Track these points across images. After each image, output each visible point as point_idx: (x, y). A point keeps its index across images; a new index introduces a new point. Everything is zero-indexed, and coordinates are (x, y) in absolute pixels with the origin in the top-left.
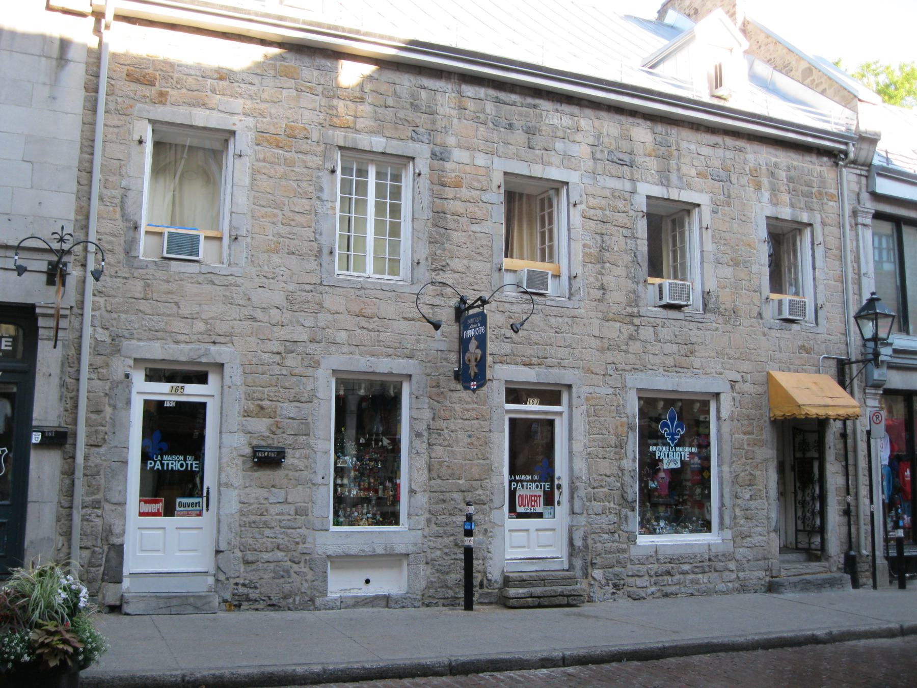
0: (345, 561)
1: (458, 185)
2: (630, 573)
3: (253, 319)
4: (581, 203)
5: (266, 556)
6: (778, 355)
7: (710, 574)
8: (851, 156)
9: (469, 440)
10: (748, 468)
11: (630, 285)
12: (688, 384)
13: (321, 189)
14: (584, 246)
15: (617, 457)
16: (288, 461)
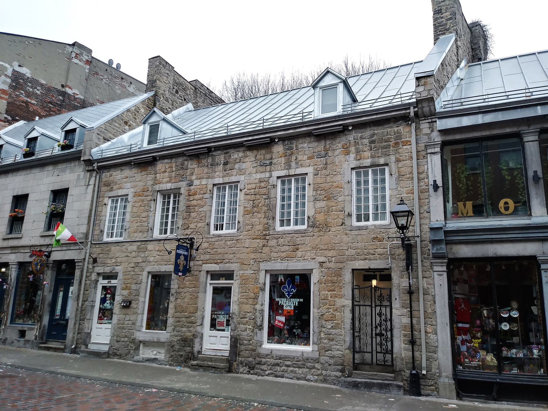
1: (195, 194)
4: (245, 189)
5: (122, 339)
6: (356, 245)
7: (304, 369)
10: (331, 310)
11: (265, 221)
12: (295, 265)
13: (151, 208)
14: (245, 207)
16: (132, 305)
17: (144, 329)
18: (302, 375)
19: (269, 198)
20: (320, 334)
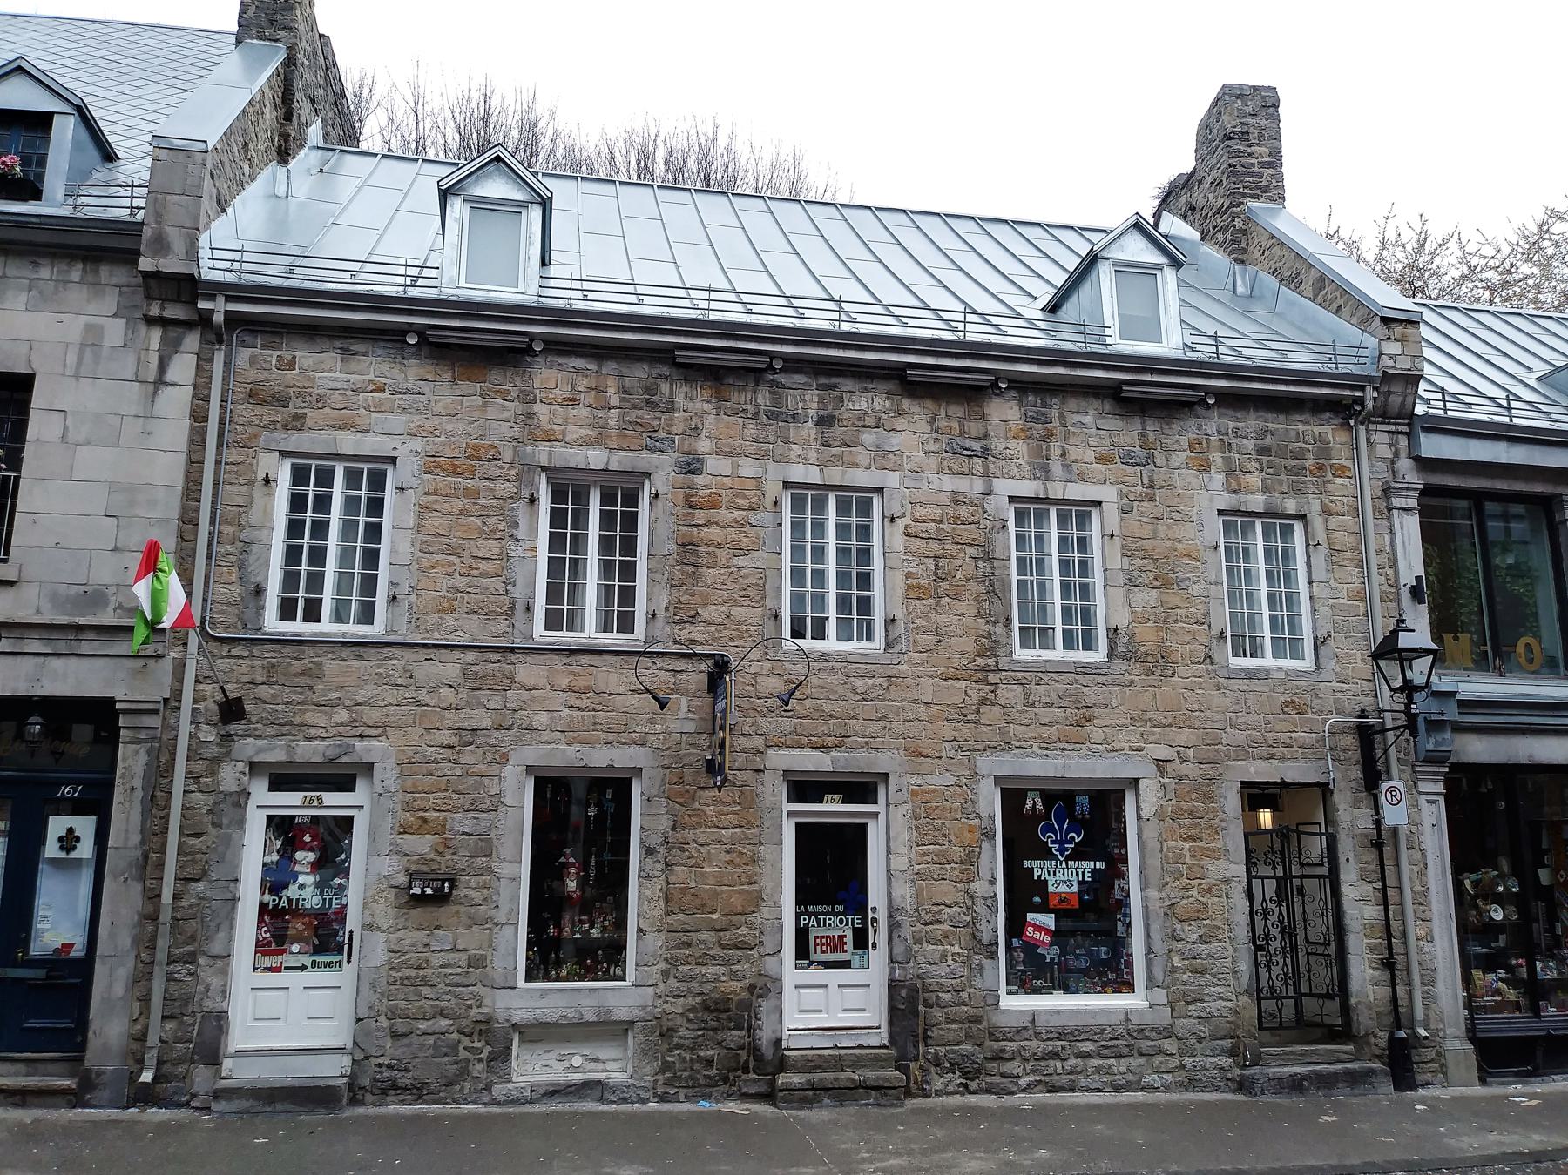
0: (539, 1033)
1: (714, 505)
2: (988, 1055)
3: (416, 702)
4: (903, 515)
5: (423, 1026)
6: (1243, 717)
7: (1131, 1060)
8: (1370, 405)
9: (728, 857)
13: (515, 525)
14: (908, 576)
15: (965, 877)
16: (461, 892)
17: (521, 982)
18: (1130, 1077)
19: (988, 557)
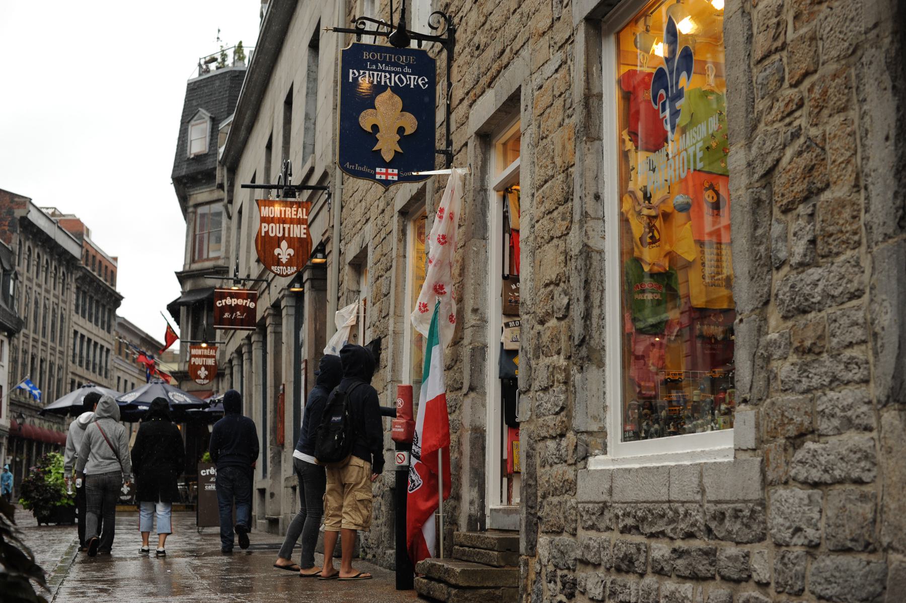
2: (578, 554)
10: (802, 119)
20: (761, 331)
